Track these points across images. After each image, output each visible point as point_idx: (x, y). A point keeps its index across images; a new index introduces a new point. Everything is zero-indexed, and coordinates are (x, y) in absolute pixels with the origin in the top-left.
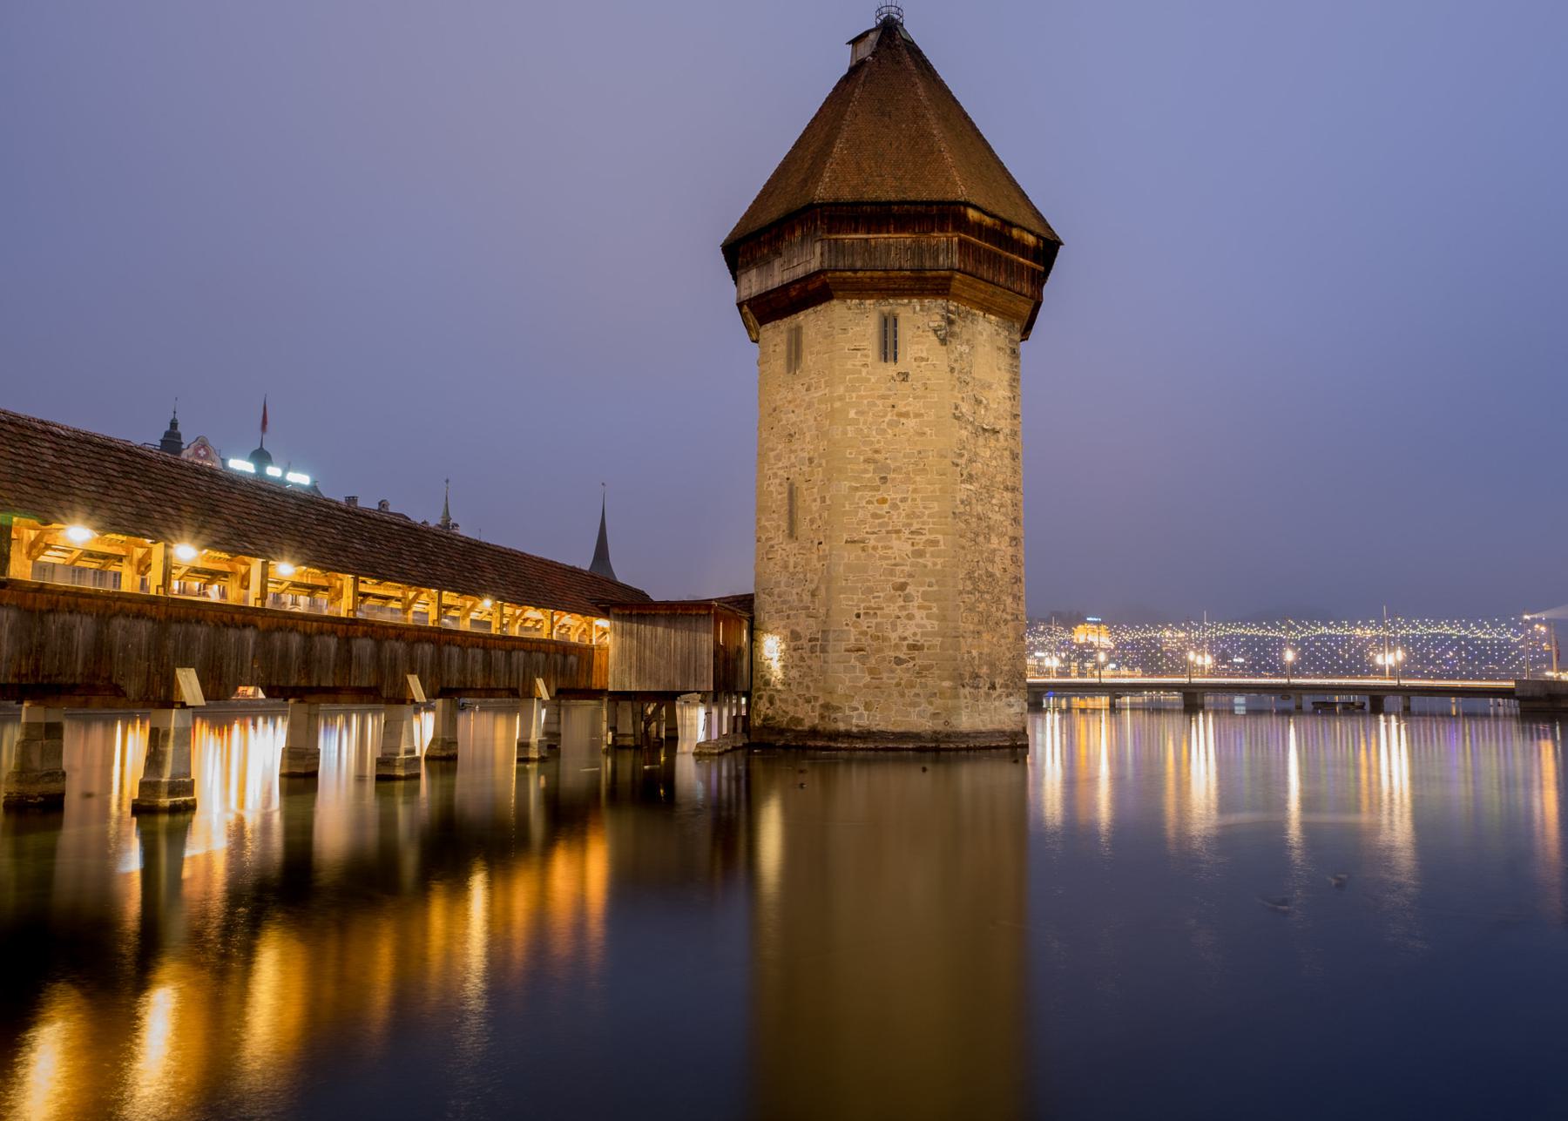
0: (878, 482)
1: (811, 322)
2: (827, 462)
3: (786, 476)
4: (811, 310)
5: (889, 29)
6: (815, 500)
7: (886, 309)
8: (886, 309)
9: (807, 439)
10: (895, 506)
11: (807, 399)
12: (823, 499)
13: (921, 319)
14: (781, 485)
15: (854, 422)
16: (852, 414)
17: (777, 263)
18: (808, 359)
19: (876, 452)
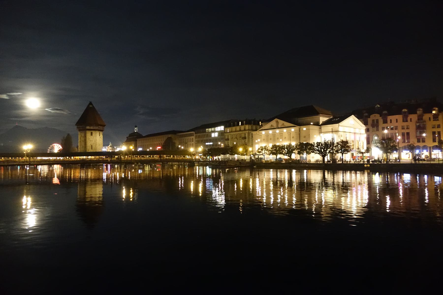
1: (93, 132)
5: (91, 103)
12: (95, 147)
18: (93, 135)
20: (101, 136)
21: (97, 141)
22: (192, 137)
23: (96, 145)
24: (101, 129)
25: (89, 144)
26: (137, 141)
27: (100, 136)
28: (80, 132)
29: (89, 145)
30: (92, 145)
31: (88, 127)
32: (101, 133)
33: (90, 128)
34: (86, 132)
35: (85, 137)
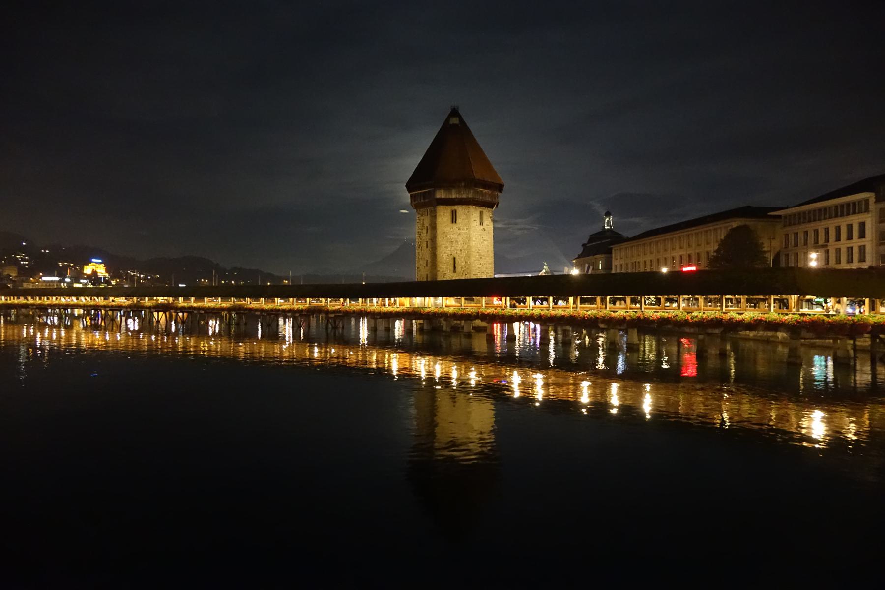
1: (460, 210)
2: (468, 252)
3: (450, 253)
5: (455, 112)
6: (463, 262)
7: (481, 210)
8: (481, 210)
9: (459, 243)
11: (459, 232)
12: (466, 262)
13: (488, 214)
15: (474, 241)
17: (454, 191)
18: (459, 220)
20: (488, 223)
21: (473, 244)
22: (855, 220)
23: (468, 256)
24: (488, 199)
25: (444, 253)
26: (611, 253)
27: (481, 223)
29: (445, 256)
30: (456, 256)
31: (441, 194)
32: (487, 214)
33: (448, 197)
34: (435, 211)
35: (433, 226)
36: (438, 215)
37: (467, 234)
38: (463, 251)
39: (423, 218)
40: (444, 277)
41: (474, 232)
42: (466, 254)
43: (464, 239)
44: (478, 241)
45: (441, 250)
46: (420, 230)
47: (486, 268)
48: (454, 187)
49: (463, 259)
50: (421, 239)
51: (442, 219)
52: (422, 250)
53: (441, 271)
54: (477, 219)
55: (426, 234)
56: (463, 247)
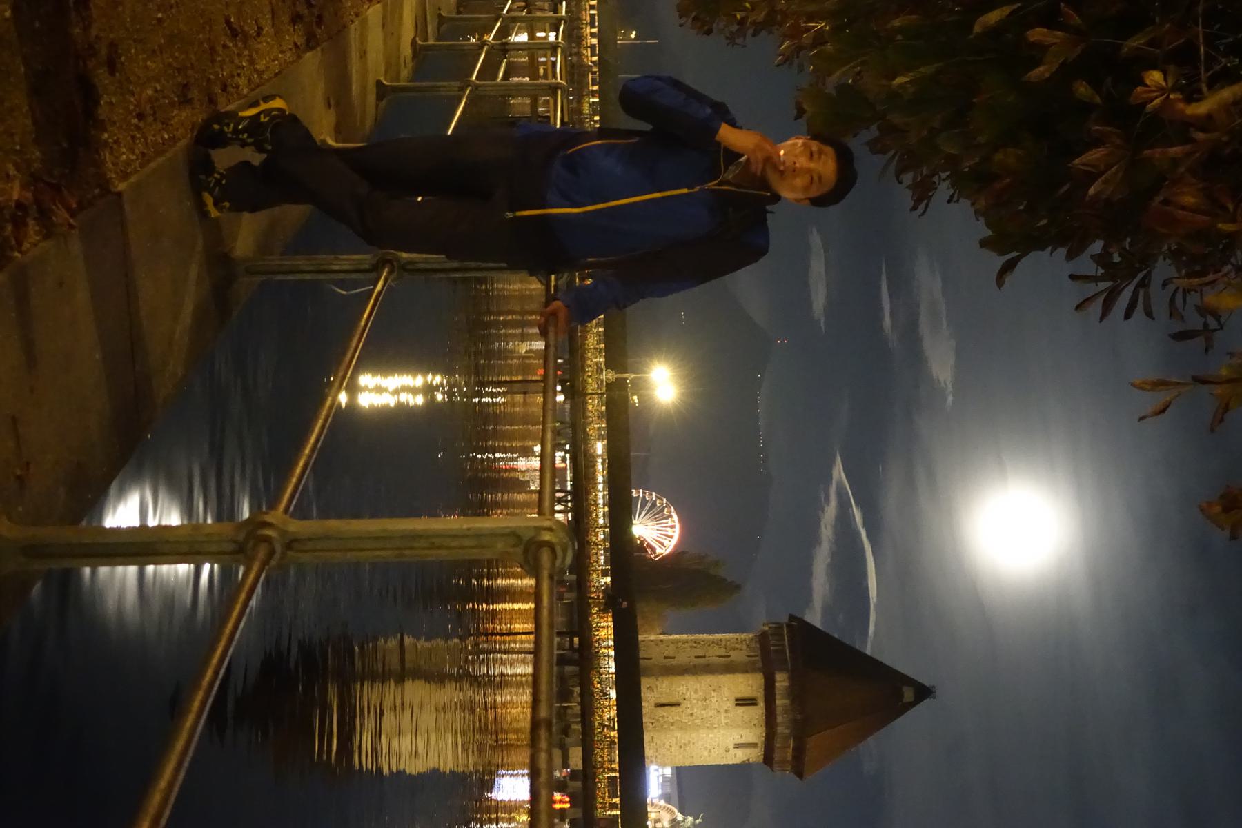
0: (679, 745)
1: (758, 712)
3: (687, 697)
4: (764, 711)
5: (923, 692)
6: (673, 718)
7: (760, 745)
8: (760, 745)
9: (703, 712)
10: (668, 750)
12: (672, 724)
14: (683, 693)
16: (711, 736)
17: (786, 702)
18: (741, 710)
19: (693, 744)
20: (738, 757)
21: (703, 734)
23: (683, 727)
24: (777, 756)
25: (687, 688)
27: (737, 746)
28: (752, 640)
29: (682, 689)
31: (782, 681)
32: (755, 755)
35: (729, 668)
36: (748, 675)
37: (719, 725)
38: (691, 718)
39: (744, 647)
40: (648, 688)
41: (723, 735)
42: (686, 723)
43: (711, 719)
44: (709, 741)
45: (692, 683)
46: (724, 643)
47: (664, 755)
48: (793, 701)
49: (678, 718)
50: (709, 645)
51: (742, 683)
52: (691, 647)
53: (658, 683)
54: (743, 737)
55: (718, 654)
56: (697, 718)
